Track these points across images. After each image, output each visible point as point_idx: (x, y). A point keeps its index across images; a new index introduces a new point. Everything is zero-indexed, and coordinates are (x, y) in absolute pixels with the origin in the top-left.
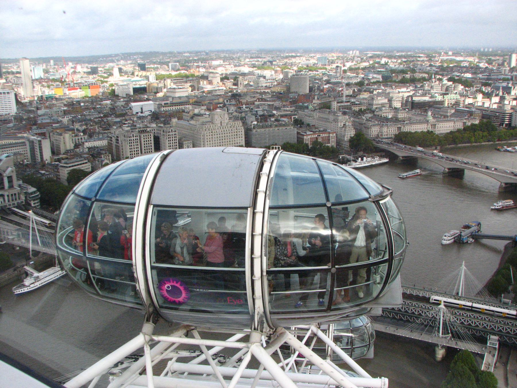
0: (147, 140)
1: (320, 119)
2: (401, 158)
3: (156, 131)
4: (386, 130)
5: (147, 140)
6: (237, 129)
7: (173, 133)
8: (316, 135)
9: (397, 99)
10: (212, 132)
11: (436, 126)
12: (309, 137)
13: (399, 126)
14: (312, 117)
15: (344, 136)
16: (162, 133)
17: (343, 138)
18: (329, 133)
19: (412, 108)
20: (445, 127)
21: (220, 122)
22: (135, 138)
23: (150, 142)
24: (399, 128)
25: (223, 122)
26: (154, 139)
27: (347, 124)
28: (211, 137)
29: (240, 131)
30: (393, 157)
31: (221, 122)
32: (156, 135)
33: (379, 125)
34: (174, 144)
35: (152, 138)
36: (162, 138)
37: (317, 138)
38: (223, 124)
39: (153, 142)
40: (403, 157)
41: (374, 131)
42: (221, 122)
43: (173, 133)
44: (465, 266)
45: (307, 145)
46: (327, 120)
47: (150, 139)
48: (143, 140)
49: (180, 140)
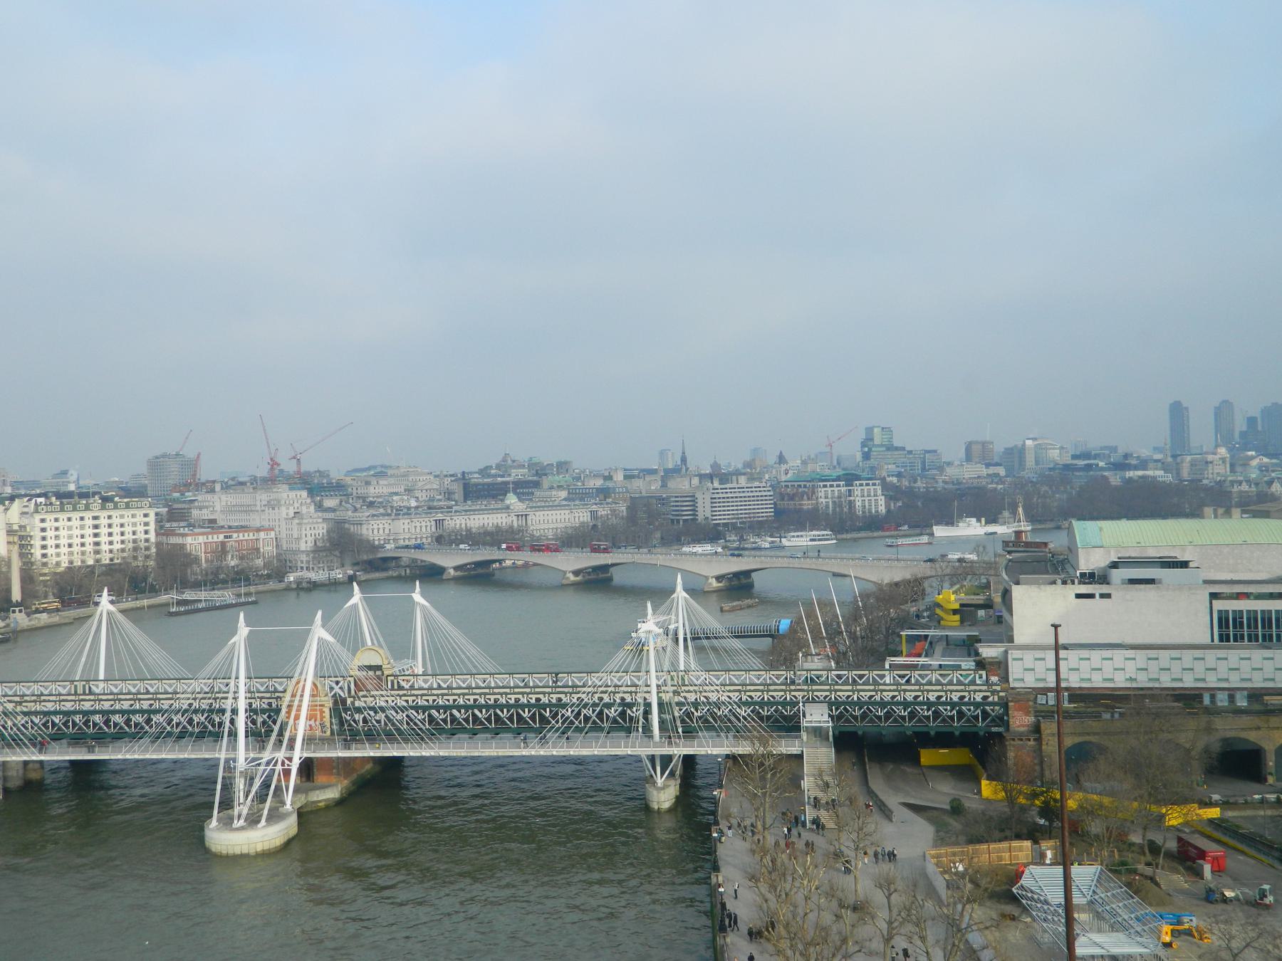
1: (229, 510)
2: (452, 571)
4: (406, 527)
8: (221, 537)
9: (428, 487)
11: (529, 518)
12: (201, 539)
13: (440, 516)
14: (207, 507)
15: (298, 539)
17: (294, 546)
18: (258, 530)
19: (466, 497)
20: (549, 520)
24: (439, 523)
27: (304, 510)
30: (431, 574)
33: (389, 515)
37: (223, 544)
40: (456, 568)
41: (376, 530)
44: (686, 590)
45: (196, 560)
46: (248, 510)
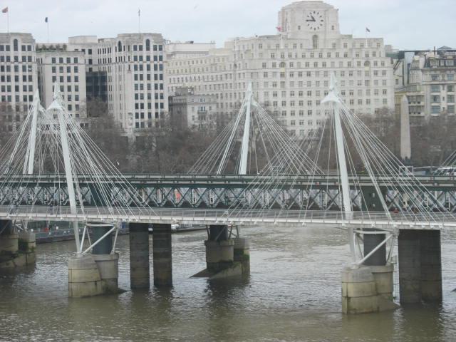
0: (65, 75)
3: (95, 57)
5: (65, 75)
6: (367, 63)
7: (152, 53)
10: (283, 65)
16: (114, 55)
21: (310, 37)
22: (20, 54)
23: (73, 84)
25: (321, 37)
26: (88, 80)
28: (278, 79)
29: (380, 69)
31: (315, 37)
32: (95, 69)
34: (153, 92)
35: (82, 75)
36: (113, 74)
38: (321, 45)
39: (82, 84)
42: (315, 37)
43: (152, 53)
47: (72, 74)
48: (48, 75)
49: (170, 98)
